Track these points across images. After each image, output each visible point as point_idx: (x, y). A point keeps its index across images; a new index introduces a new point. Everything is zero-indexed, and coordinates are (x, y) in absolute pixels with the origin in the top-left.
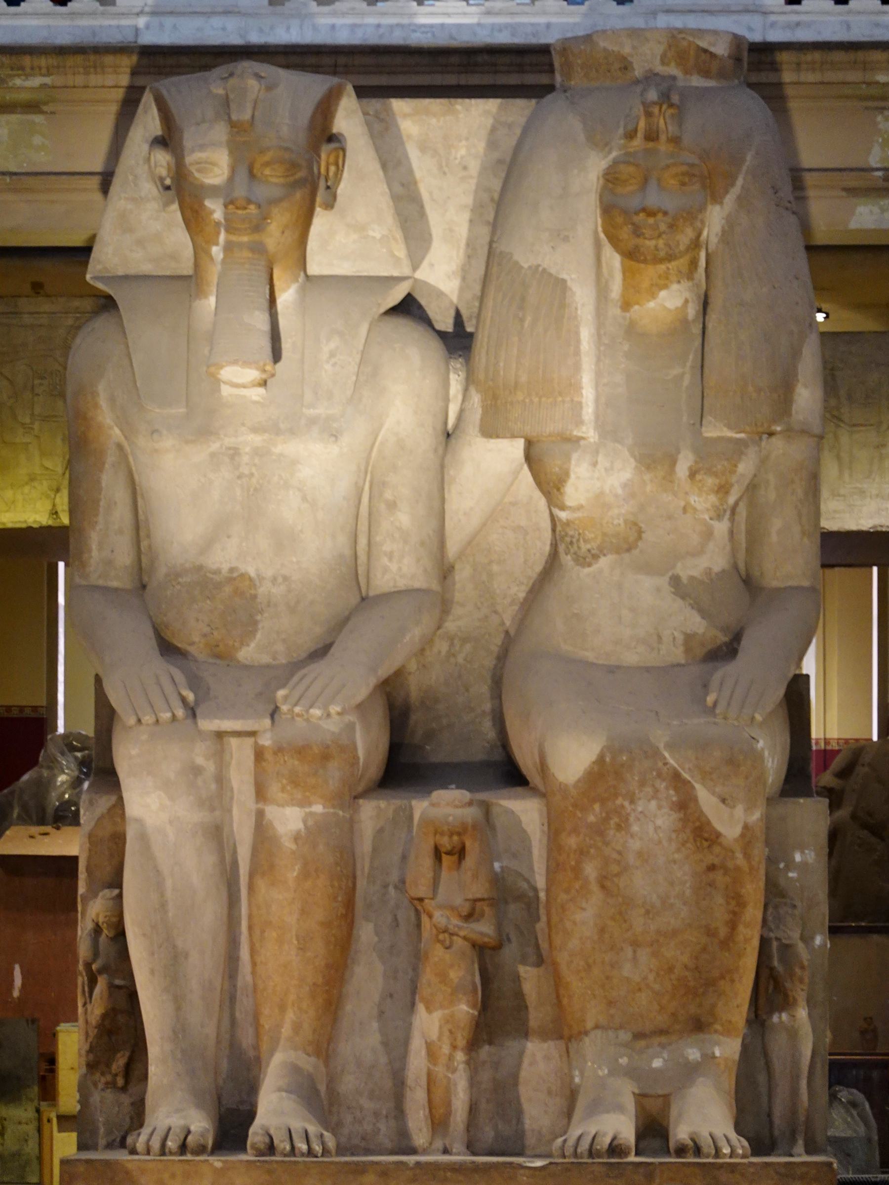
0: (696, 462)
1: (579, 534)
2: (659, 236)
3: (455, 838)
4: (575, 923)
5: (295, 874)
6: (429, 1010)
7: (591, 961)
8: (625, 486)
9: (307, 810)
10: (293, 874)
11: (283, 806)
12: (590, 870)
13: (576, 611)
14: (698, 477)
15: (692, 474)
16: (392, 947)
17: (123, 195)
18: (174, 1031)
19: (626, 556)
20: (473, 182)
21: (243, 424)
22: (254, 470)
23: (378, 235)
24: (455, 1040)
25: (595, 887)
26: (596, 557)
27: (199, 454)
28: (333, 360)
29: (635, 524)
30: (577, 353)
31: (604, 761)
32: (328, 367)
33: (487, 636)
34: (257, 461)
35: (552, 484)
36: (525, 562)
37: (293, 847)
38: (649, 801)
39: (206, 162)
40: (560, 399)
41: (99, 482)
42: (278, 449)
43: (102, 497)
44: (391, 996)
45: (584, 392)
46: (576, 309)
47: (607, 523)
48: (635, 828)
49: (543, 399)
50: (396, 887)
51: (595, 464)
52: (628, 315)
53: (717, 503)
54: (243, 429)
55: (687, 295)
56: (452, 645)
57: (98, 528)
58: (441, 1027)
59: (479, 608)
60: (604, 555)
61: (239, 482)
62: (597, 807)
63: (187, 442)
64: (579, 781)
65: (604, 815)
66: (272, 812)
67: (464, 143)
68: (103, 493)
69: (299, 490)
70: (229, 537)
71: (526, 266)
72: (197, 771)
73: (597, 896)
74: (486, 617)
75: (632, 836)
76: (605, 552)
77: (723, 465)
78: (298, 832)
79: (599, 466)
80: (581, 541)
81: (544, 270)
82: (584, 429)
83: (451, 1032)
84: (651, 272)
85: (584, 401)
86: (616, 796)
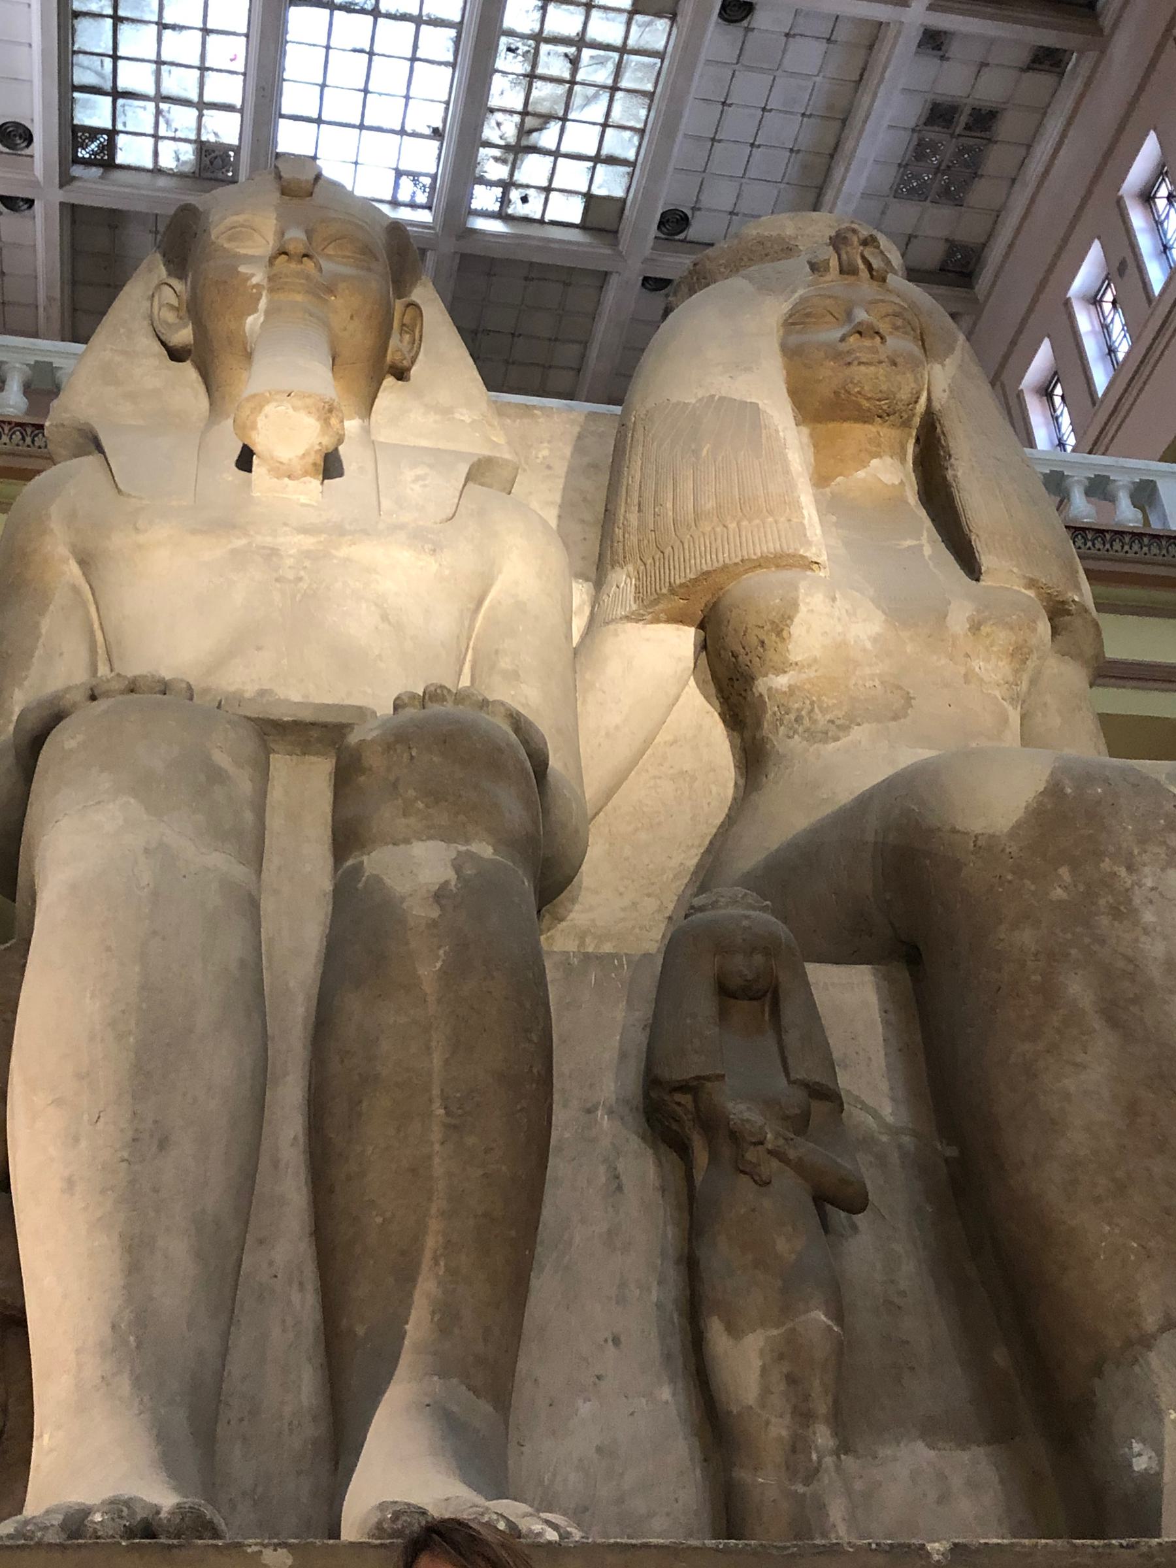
0: (978, 611)
1: (812, 703)
2: (880, 362)
3: (758, 959)
4: (1067, 1097)
5: (438, 965)
6: (733, 1330)
7: (1119, 1174)
8: (875, 640)
9: (462, 848)
10: (428, 971)
11: (407, 841)
12: (1078, 989)
13: (825, 796)
14: (985, 629)
15: (975, 627)
16: (611, 1234)
17: (109, 346)
18: (114, 1327)
19: (892, 724)
20: (560, 483)
21: (285, 524)
22: (302, 573)
23: (468, 421)
24: (807, 1397)
25: (1097, 1023)
26: (845, 728)
27: (213, 550)
28: (421, 483)
29: (899, 687)
30: (787, 472)
31: (1062, 790)
32: (417, 487)
33: (637, 930)
34: (307, 563)
35: (768, 627)
36: (693, 818)
37: (435, 913)
38: (1163, 870)
39: (242, 226)
40: (770, 519)
41: (37, 625)
42: (343, 552)
43: (40, 644)
44: (616, 1341)
45: (805, 512)
46: (777, 431)
47: (855, 685)
48: (1148, 917)
49: (745, 523)
50: (610, 1112)
51: (834, 599)
52: (828, 490)
53: (1011, 679)
54: (285, 529)
55: (902, 476)
56: (582, 943)
57: (26, 683)
58: (764, 1370)
59: (621, 894)
60: (859, 725)
61: (278, 585)
62: (1064, 871)
63: (194, 532)
64: (1018, 825)
65: (1082, 888)
66: (377, 862)
67: (546, 444)
68: (41, 641)
69: (376, 605)
70: (259, 648)
71: (693, 401)
72: (216, 776)
73: (1104, 1040)
74: (634, 904)
75: (1146, 932)
76: (859, 720)
77: (1019, 616)
78: (447, 883)
79: (838, 603)
80: (816, 709)
81: (722, 399)
82: (814, 550)
83: (792, 1380)
84: (858, 432)
85: (806, 522)
86: (1098, 855)
